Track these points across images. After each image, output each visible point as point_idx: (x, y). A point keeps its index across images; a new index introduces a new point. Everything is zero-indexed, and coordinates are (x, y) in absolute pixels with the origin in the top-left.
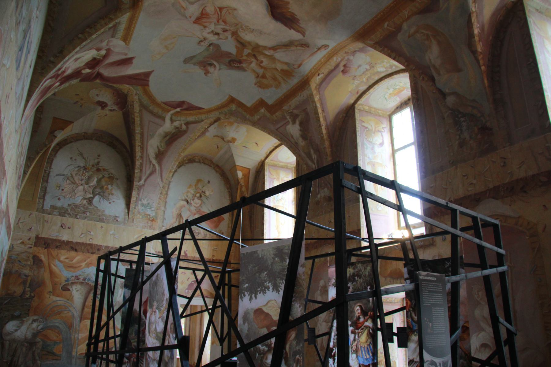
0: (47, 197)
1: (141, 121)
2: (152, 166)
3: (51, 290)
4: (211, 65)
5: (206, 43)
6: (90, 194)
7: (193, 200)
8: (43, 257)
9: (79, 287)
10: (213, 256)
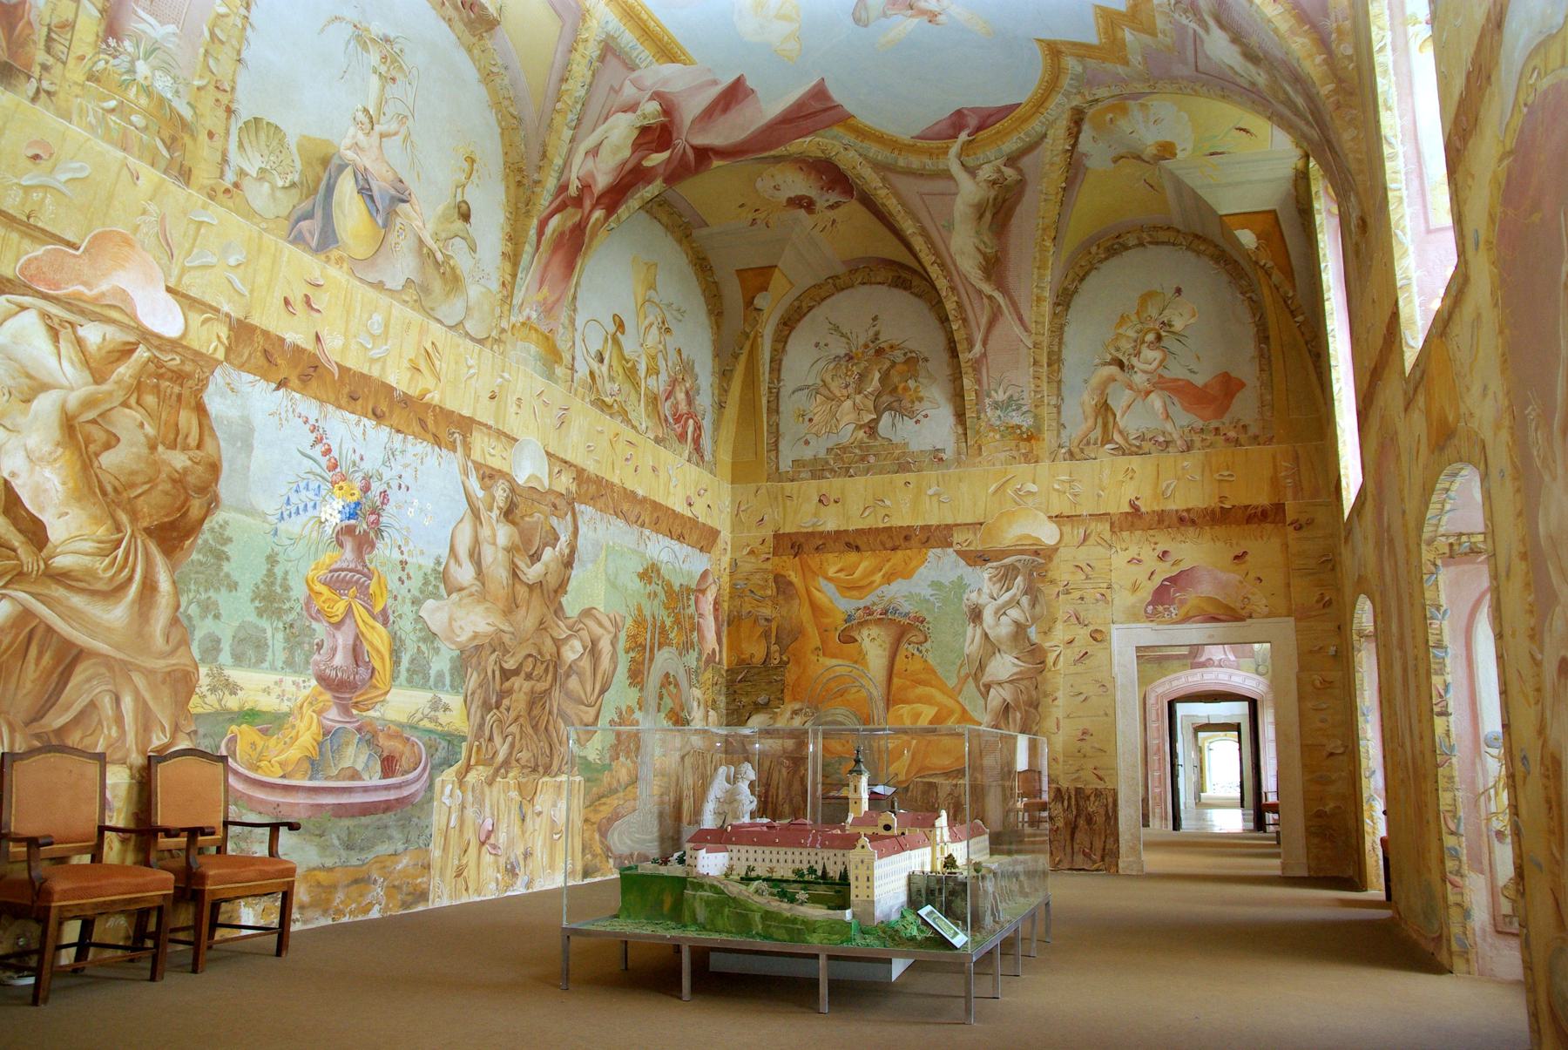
0: (783, 445)
2: (985, 300)
3: (816, 642)
6: (869, 412)
7: (1138, 354)
8: (794, 577)
9: (874, 631)
10: (1222, 498)
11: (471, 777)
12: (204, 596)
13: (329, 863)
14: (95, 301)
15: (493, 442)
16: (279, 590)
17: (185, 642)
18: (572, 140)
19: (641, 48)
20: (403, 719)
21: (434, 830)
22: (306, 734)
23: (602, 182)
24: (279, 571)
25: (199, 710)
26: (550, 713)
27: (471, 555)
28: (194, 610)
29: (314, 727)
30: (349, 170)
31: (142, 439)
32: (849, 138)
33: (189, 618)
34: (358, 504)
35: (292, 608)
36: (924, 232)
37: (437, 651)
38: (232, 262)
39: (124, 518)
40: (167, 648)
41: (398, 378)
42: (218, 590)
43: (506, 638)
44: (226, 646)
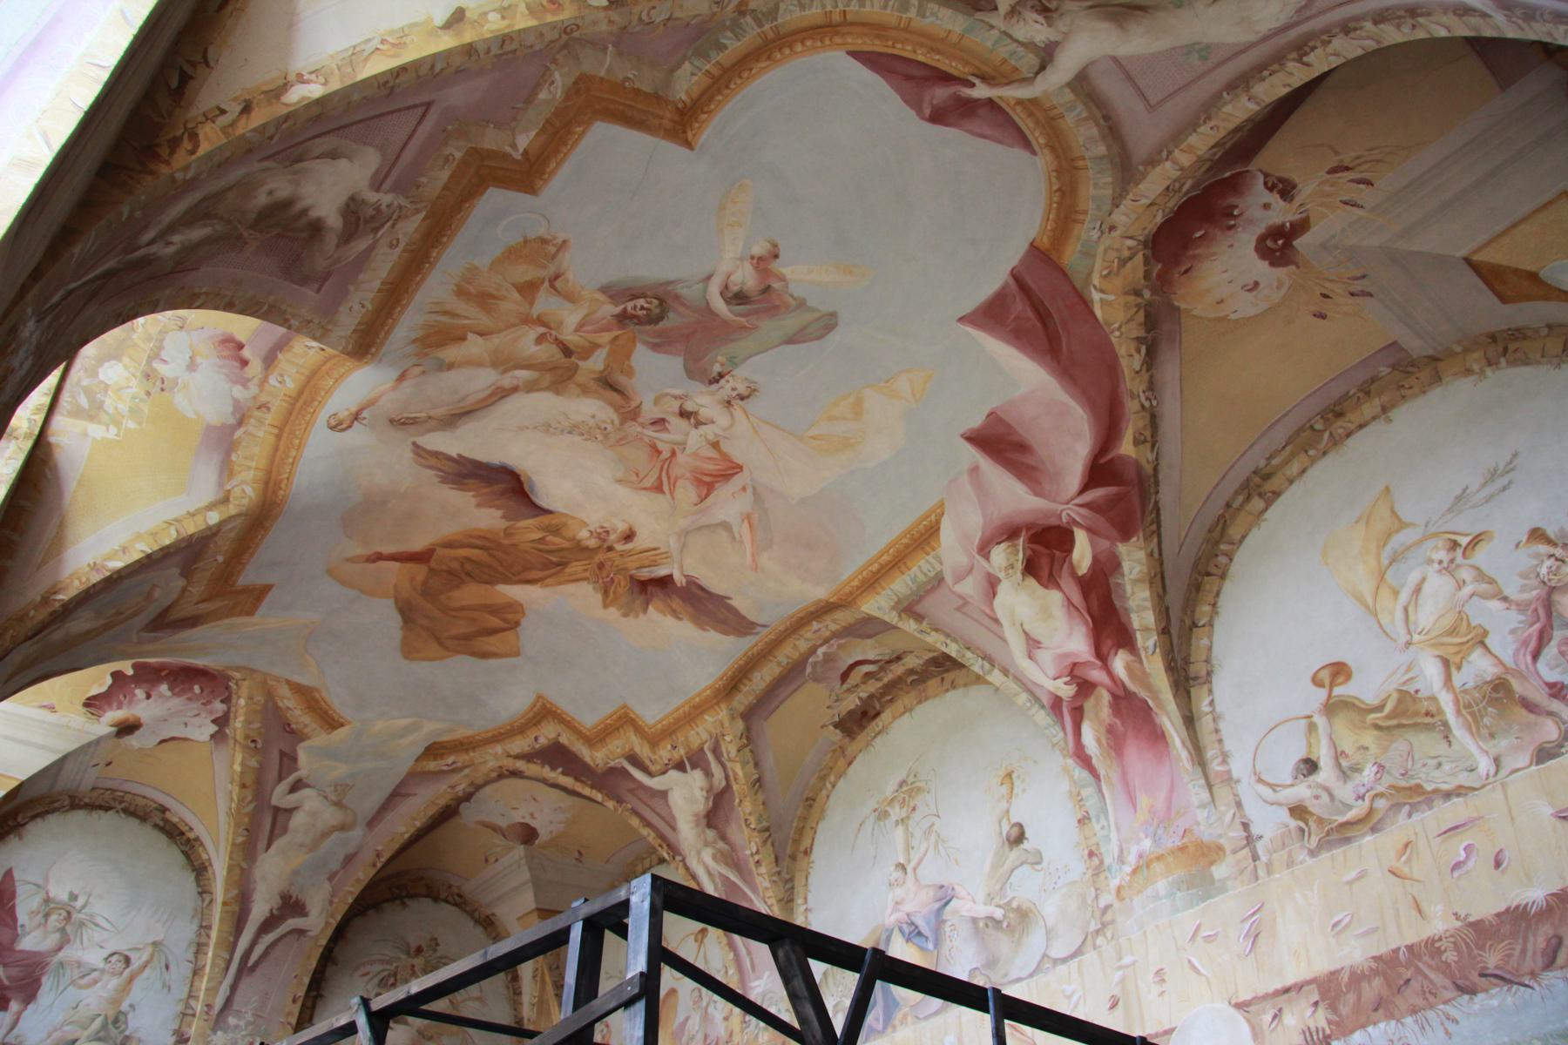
1: (1193, 126)
4: (738, 298)
5: (728, 387)
18: (1006, 672)
19: (915, 569)
23: (1076, 642)
30: (896, 934)
32: (1086, 231)
36: (1242, 82)
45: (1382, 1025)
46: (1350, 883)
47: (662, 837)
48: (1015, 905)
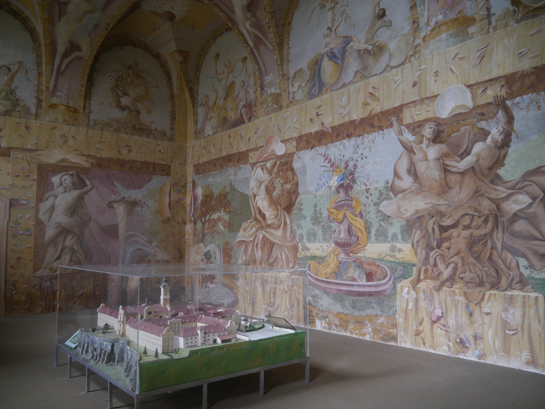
11: (422, 285)
12: (298, 223)
13: (346, 312)
14: (268, 156)
15: (418, 108)
16: (319, 215)
17: (294, 237)
20: (375, 256)
21: (398, 308)
22: (333, 264)
24: (318, 209)
25: (300, 257)
26: (493, 248)
27: (409, 172)
28: (296, 228)
29: (335, 261)
31: (280, 185)
33: (295, 230)
34: (344, 174)
35: (323, 220)
37: (391, 224)
38: (295, 121)
39: (279, 207)
40: (291, 240)
41: (356, 116)
42: (301, 220)
43: (442, 209)
44: (305, 237)
45: (530, 95)
46: (532, 35)
47: (228, 16)
48: (377, 44)
